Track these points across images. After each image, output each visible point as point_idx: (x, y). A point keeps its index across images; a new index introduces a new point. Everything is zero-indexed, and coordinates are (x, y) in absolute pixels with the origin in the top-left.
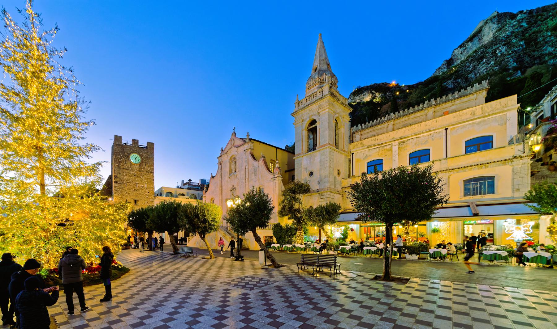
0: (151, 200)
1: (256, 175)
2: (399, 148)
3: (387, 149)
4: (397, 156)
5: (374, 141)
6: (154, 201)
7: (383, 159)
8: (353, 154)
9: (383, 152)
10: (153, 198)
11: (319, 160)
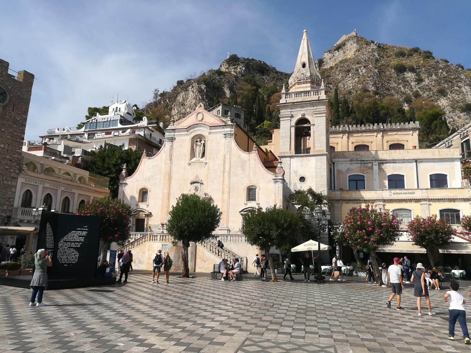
0: (12, 175)
1: (243, 170)
2: (379, 168)
4: (378, 175)
5: (355, 155)
6: (17, 179)
7: (365, 175)
8: (334, 163)
9: (365, 169)
10: (17, 172)
11: (314, 165)
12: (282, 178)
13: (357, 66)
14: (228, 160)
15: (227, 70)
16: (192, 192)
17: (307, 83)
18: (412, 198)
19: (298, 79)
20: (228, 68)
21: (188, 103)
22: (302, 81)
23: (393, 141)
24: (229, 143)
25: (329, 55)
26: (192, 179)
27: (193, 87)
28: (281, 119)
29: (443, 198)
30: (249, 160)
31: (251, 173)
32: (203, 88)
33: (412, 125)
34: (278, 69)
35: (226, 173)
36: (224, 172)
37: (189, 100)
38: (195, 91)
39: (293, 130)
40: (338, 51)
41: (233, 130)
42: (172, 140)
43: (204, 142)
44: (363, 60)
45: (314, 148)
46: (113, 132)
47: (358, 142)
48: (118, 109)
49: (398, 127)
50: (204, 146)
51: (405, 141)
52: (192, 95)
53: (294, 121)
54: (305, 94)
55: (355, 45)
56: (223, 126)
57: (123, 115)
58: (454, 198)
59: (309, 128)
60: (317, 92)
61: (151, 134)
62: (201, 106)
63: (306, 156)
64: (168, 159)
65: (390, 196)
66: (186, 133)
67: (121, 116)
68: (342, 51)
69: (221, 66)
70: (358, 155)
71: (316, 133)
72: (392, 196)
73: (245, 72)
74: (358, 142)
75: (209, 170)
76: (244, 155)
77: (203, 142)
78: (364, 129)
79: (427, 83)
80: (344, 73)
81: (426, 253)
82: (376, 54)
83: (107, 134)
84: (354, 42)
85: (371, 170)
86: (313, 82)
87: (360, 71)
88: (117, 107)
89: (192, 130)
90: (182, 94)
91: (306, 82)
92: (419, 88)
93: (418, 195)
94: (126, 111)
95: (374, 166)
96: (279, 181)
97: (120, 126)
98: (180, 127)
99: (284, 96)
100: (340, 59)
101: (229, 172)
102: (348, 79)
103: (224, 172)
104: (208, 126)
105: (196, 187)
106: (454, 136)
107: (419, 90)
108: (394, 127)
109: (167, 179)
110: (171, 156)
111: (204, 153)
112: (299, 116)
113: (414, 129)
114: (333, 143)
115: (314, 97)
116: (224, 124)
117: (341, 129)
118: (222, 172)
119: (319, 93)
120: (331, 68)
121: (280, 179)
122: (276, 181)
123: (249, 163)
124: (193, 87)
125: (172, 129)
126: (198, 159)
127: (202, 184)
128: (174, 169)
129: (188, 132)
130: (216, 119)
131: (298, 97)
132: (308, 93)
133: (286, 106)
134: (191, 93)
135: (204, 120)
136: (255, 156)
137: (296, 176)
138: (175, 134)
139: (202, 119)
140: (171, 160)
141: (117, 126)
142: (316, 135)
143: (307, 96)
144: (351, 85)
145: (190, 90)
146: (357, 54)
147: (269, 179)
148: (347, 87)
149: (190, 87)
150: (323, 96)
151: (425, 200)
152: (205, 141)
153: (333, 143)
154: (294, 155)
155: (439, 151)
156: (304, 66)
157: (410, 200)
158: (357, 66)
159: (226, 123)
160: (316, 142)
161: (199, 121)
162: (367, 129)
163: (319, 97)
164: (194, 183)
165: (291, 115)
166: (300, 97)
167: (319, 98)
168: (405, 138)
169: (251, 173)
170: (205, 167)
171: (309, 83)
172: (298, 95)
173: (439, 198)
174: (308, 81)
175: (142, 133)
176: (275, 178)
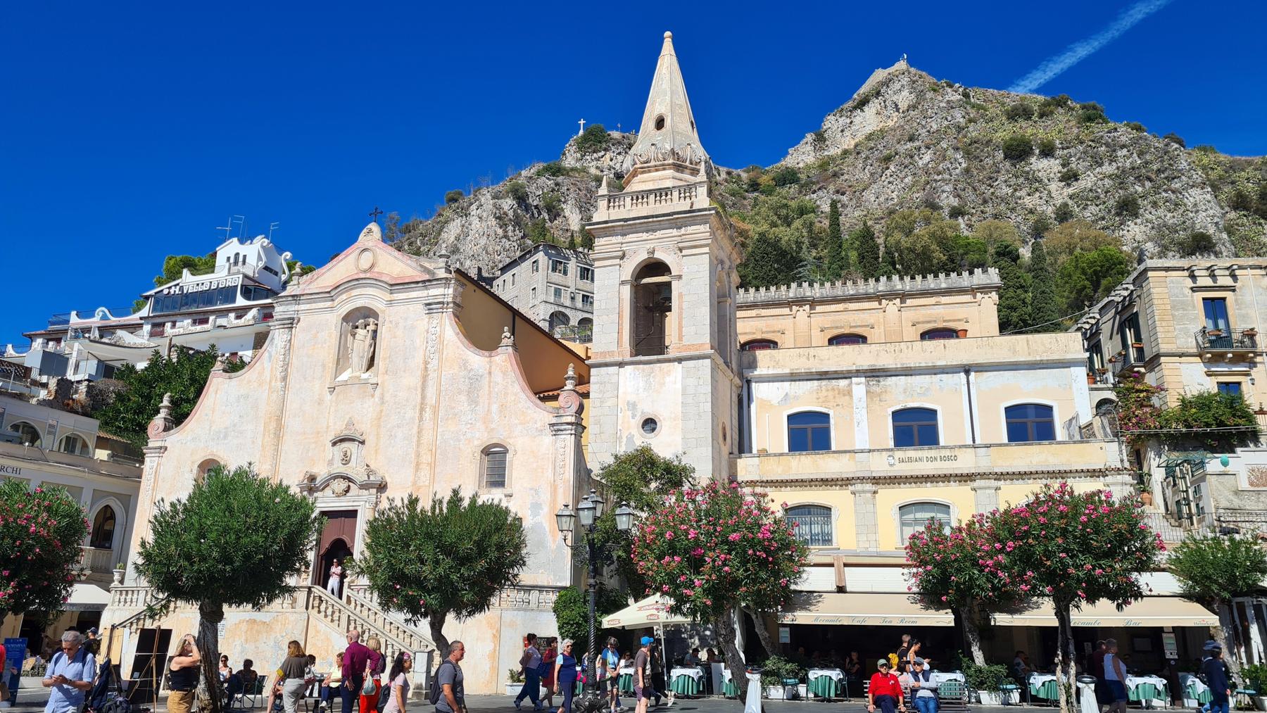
1: (474, 402)
3: (839, 390)
4: (865, 411)
5: (804, 359)
9: (830, 394)
11: (679, 386)
12: (572, 419)
13: (909, 145)
14: (432, 375)
15: (578, 165)
16: (335, 466)
17: (664, 169)
18: (948, 472)
19: (642, 160)
22: (653, 163)
24: (438, 329)
25: (841, 120)
26: (338, 429)
28: (597, 264)
29: (1033, 470)
30: (490, 373)
31: (495, 408)
32: (506, 208)
33: (979, 277)
35: (427, 410)
36: (422, 410)
37: (469, 238)
39: (627, 291)
41: (451, 291)
42: (292, 324)
45: (680, 338)
46: (212, 318)
47: (837, 328)
48: (241, 259)
49: (944, 285)
50: (374, 338)
53: (629, 268)
55: (905, 93)
56: (424, 282)
57: (251, 274)
58: (1062, 469)
60: (688, 189)
62: (370, 231)
63: (659, 361)
64: (279, 377)
65: (890, 468)
66: (329, 304)
67: (246, 276)
70: (812, 359)
71: (685, 298)
72: (895, 468)
74: (837, 328)
75: (383, 403)
76: (477, 359)
77: (371, 327)
78: (851, 292)
79: (1089, 185)
81: (953, 624)
85: (847, 397)
86: (680, 166)
88: (237, 254)
89: (344, 296)
91: (663, 165)
92: (1071, 197)
93: (966, 462)
94: (261, 264)
95: (854, 387)
96: (565, 430)
97: (241, 301)
98: (313, 288)
99: (603, 204)
100: (868, 130)
101: (435, 410)
102: (888, 180)
103: (422, 410)
104: (386, 283)
105: (345, 455)
107: (1070, 202)
108: (932, 286)
109: (272, 431)
110: (286, 370)
111: (372, 358)
112: (642, 256)
113: (985, 289)
114: (774, 332)
115: (677, 204)
116: (427, 277)
117: (791, 295)
118: (418, 407)
119: (694, 194)
120: (846, 152)
121: (568, 424)
122: (556, 429)
123: (490, 382)
125: (293, 296)
126: (358, 374)
127: (363, 443)
128: (292, 404)
129: (333, 300)
130: (408, 265)
131: (640, 205)
132: (666, 195)
133: (609, 229)
134: (475, 222)
135: (376, 269)
136: (506, 361)
137: (633, 418)
138: (302, 307)
139: (372, 266)
140: (284, 379)
141: (234, 301)
143: (663, 202)
144: (894, 195)
147: (539, 425)
149: (474, 207)
150: (702, 200)
151: (983, 476)
152: (377, 325)
153: (774, 332)
154: (628, 358)
155: (1028, 341)
156: (660, 123)
157: (946, 478)
158: (908, 146)
159: (434, 273)
161: (365, 271)
162: (861, 291)
163: (692, 204)
164: (342, 440)
165: (620, 253)
166: (645, 205)
167: (691, 207)
168: (960, 312)
169: (495, 408)
170: (373, 396)
171: (670, 169)
172: (640, 200)
173: (1022, 470)
174: (666, 162)
176: (554, 421)
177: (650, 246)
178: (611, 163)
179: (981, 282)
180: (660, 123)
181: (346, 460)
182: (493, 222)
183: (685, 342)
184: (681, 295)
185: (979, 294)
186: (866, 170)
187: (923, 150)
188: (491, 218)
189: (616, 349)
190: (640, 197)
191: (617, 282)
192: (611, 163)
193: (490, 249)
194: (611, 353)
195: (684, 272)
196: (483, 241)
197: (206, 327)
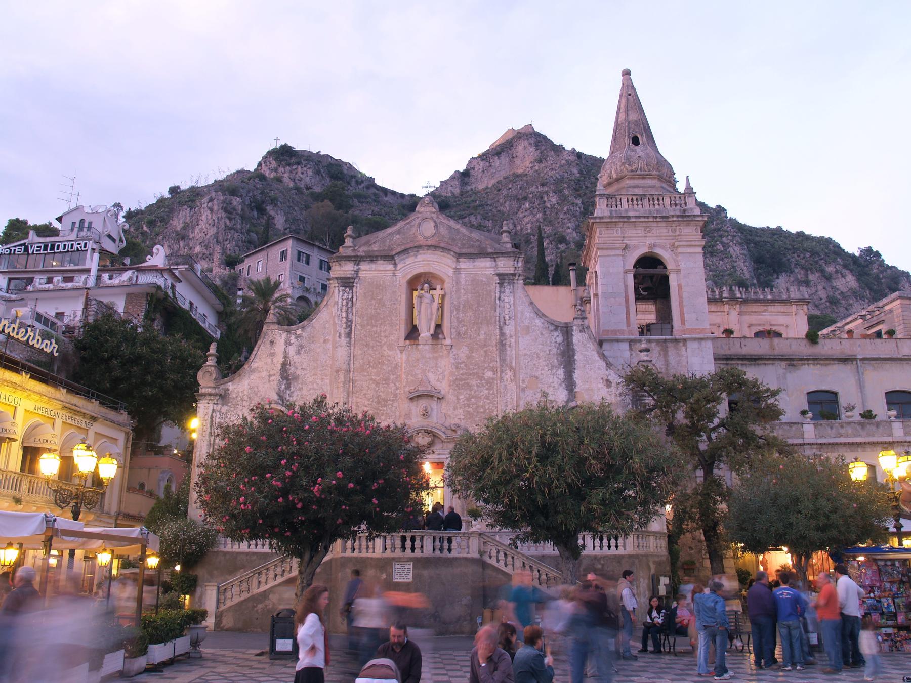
13: (540, 189)
20: (276, 170)
21: (197, 233)
22: (639, 172)
23: (760, 325)
25: (482, 164)
27: (211, 200)
34: (378, 182)
37: (200, 227)
38: (215, 208)
40: (499, 158)
41: (520, 264)
43: (442, 292)
44: (551, 179)
45: (683, 322)
48: (86, 225)
49: (769, 297)
51: (783, 325)
52: (209, 217)
54: (651, 202)
55: (533, 149)
59: (665, 279)
61: (173, 287)
68: (507, 159)
69: (260, 165)
73: (313, 181)
80: (514, 203)
82: (575, 171)
83: (68, 280)
84: (530, 144)
87: (545, 199)
88: (82, 221)
90: (184, 213)
106: (847, 324)
108: (762, 297)
110: (350, 327)
124: (211, 200)
134: (205, 215)
141: (84, 265)
142: (685, 295)
144: (529, 226)
145: (205, 206)
146: (536, 168)
148: (522, 229)
149: (205, 200)
160: (685, 309)
165: (624, 246)
172: (635, 202)
175: (160, 282)
177: (648, 242)
178: (301, 176)
179: (797, 297)
180: (635, 141)
181: (426, 414)
182: (224, 215)
183: (688, 326)
184: (680, 287)
185: (794, 307)
186: (506, 205)
187: (551, 194)
188: (221, 211)
189: (625, 328)
190: (635, 199)
191: (621, 270)
192: (301, 176)
193: (220, 238)
194: (623, 332)
195: (682, 266)
196: (212, 231)
197: (70, 285)
